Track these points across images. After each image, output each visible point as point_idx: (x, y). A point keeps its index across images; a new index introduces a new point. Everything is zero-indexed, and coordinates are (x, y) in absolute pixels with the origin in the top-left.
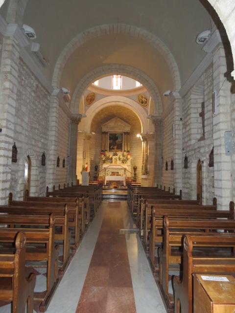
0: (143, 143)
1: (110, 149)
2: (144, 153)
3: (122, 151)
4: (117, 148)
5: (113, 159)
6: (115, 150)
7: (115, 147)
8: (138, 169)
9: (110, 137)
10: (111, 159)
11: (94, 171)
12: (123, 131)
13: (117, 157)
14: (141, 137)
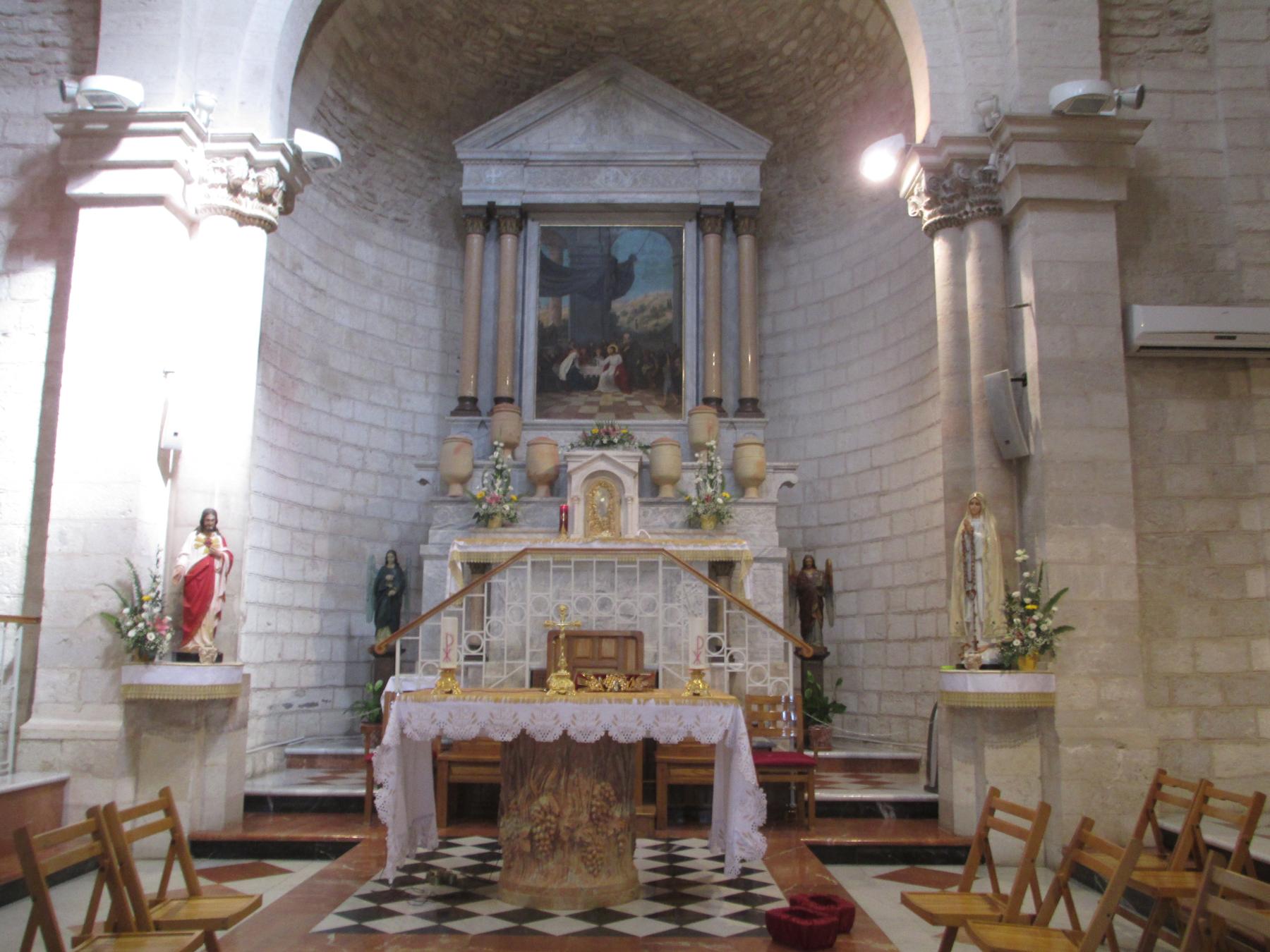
0: (940, 248)
1: (548, 384)
2: (960, 371)
3: (674, 407)
4: (627, 380)
5: (576, 485)
6: (608, 395)
7: (606, 367)
8: (843, 603)
9: (546, 266)
10: (555, 483)
11: (365, 626)
12: (693, 199)
13: (623, 460)
14: (914, 178)
